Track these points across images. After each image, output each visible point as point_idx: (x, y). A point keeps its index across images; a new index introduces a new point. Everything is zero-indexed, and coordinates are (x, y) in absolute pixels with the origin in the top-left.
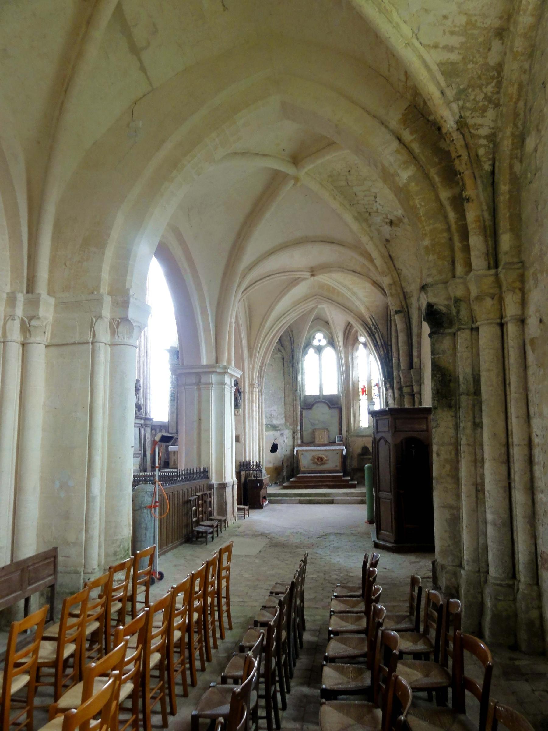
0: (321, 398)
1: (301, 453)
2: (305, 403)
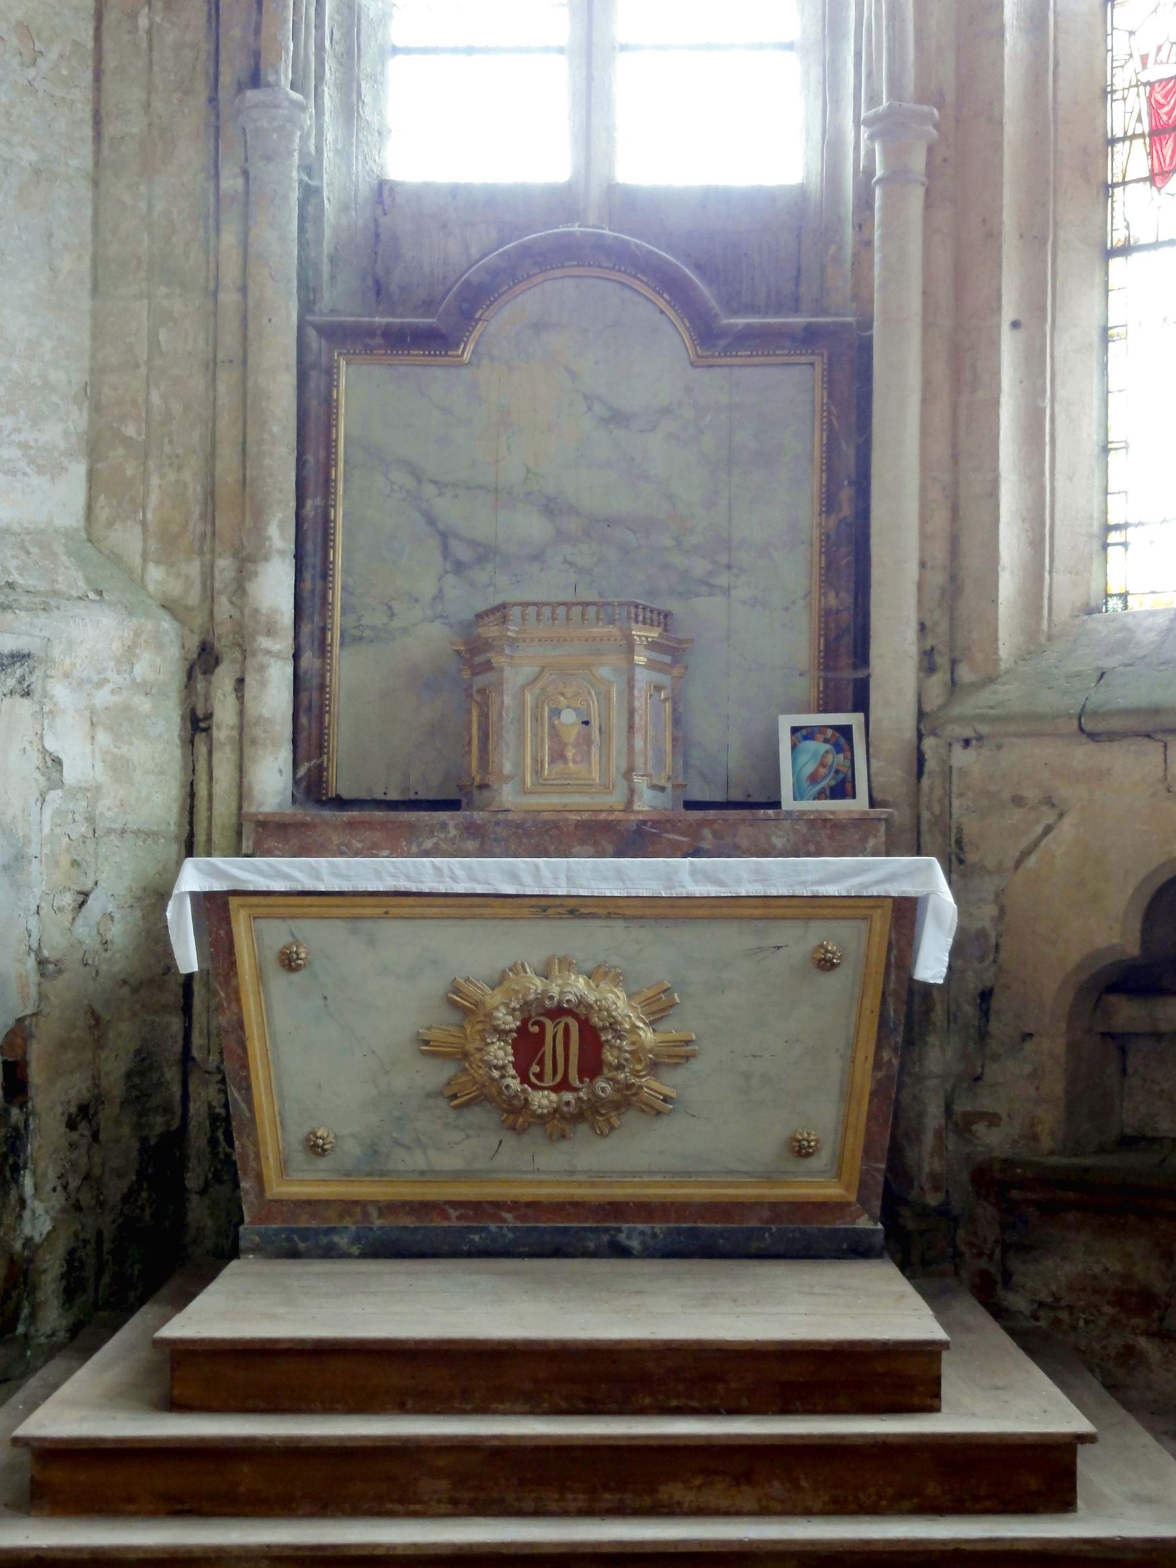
1: (277, 935)
2: (379, 289)
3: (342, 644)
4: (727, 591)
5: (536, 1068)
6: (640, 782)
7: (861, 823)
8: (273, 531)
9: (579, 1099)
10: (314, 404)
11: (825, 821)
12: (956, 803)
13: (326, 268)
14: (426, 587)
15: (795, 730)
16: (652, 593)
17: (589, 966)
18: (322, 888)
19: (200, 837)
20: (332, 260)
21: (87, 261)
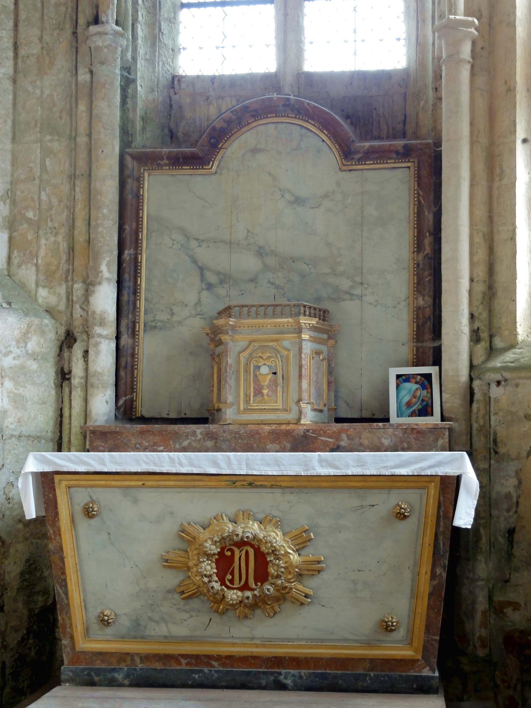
0: (287, 89)
2: (172, 135)
3: (145, 331)
4: (361, 297)
5: (229, 577)
6: (307, 409)
7: (435, 429)
8: (104, 268)
9: (254, 596)
10: (129, 197)
11: (413, 429)
12: (493, 418)
13: (139, 124)
14: (191, 298)
15: (398, 376)
16: (319, 299)
17: (261, 516)
18: (106, 470)
19: (65, 439)
20: (143, 119)
21: (10, 123)
